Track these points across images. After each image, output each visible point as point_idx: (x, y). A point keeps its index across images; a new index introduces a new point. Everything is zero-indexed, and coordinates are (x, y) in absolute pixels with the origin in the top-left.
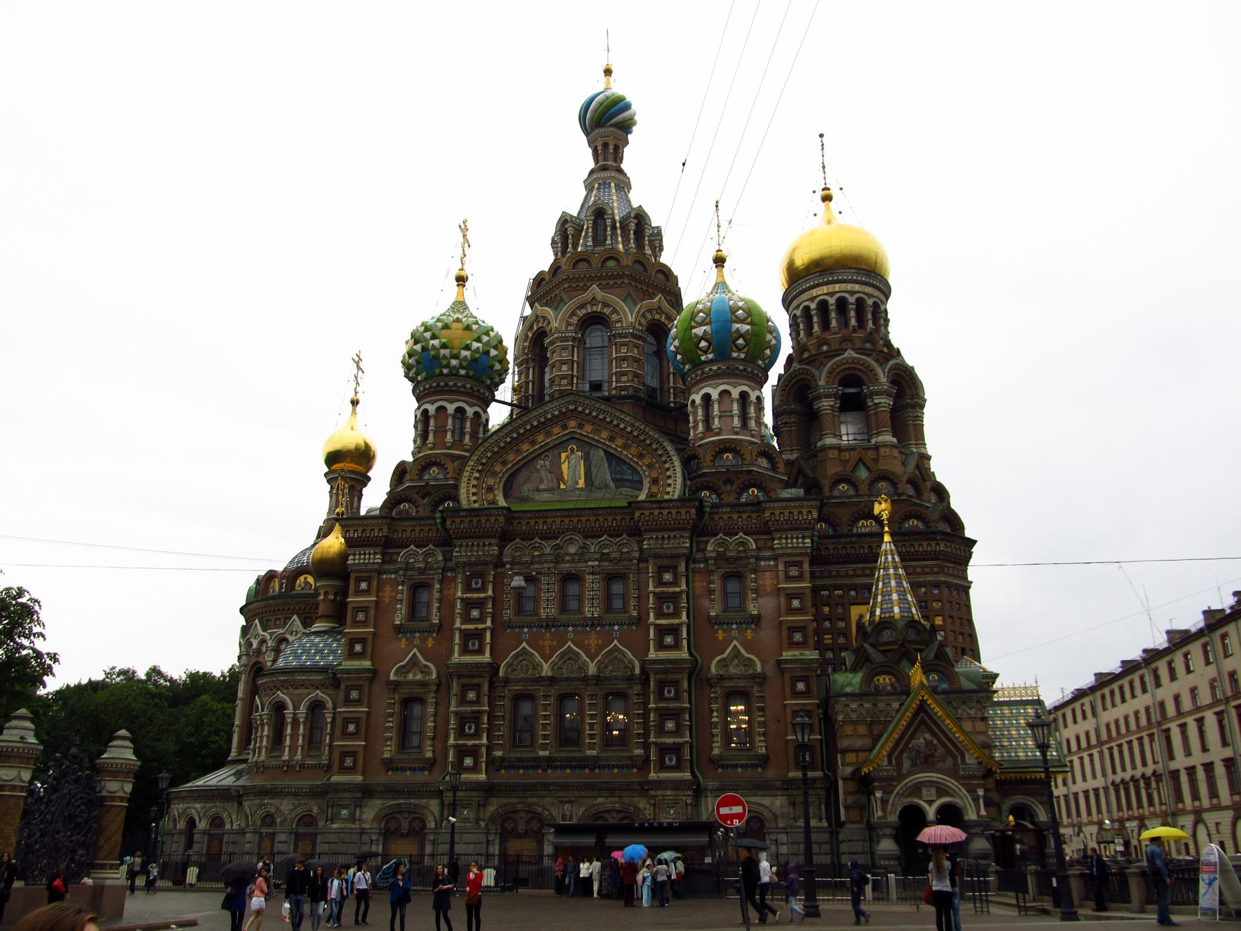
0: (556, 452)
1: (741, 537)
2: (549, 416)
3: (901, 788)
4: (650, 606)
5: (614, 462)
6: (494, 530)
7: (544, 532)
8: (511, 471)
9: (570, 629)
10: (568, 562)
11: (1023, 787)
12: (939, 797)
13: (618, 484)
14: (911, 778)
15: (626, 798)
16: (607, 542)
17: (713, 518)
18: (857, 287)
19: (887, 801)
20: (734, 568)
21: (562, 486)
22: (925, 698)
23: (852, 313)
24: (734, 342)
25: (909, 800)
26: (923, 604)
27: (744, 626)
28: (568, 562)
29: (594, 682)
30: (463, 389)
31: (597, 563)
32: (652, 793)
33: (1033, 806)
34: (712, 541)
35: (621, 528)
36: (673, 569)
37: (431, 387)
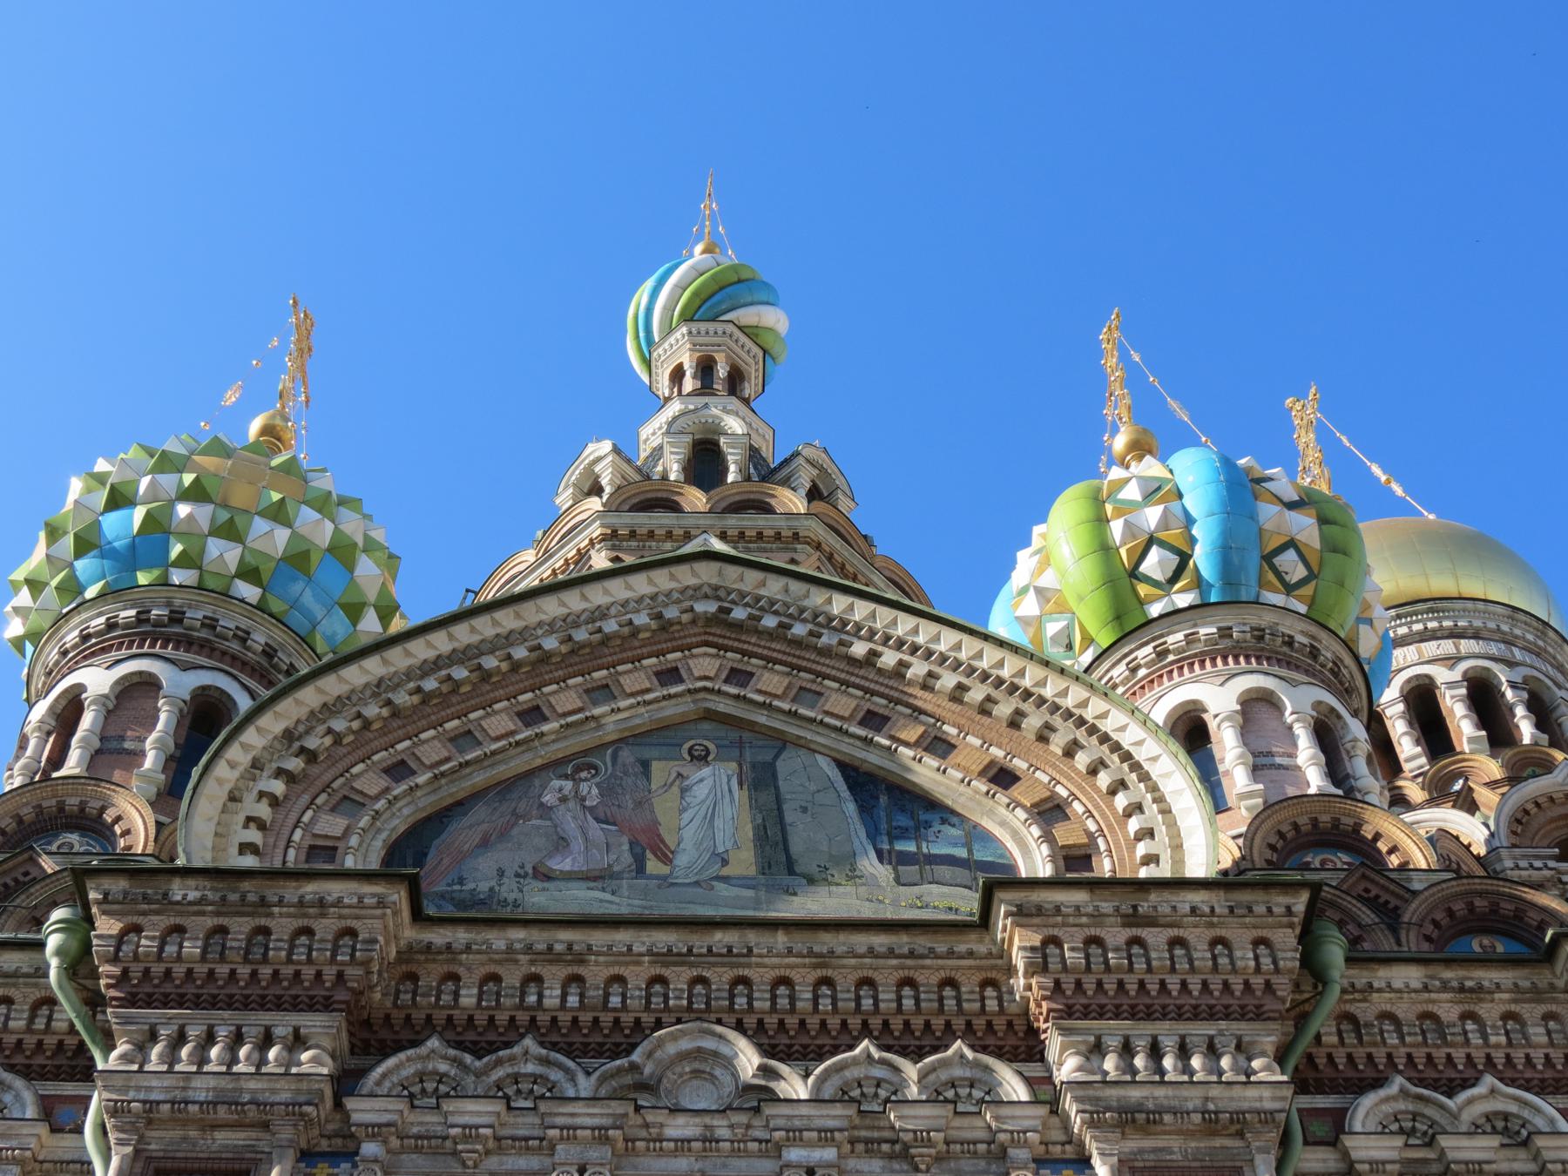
0: (627, 755)
1: (1493, 1091)
2: (610, 626)
5: (883, 800)
6: (330, 973)
7: (564, 1018)
8: (426, 803)
10: (683, 1144)
13: (910, 871)
17: (1351, 1018)
18: (1518, 654)
21: (653, 866)
23: (1520, 711)
24: (1268, 558)
30: (235, 646)
31: (829, 1154)
34: (1368, 1100)
35: (938, 1023)
37: (111, 626)
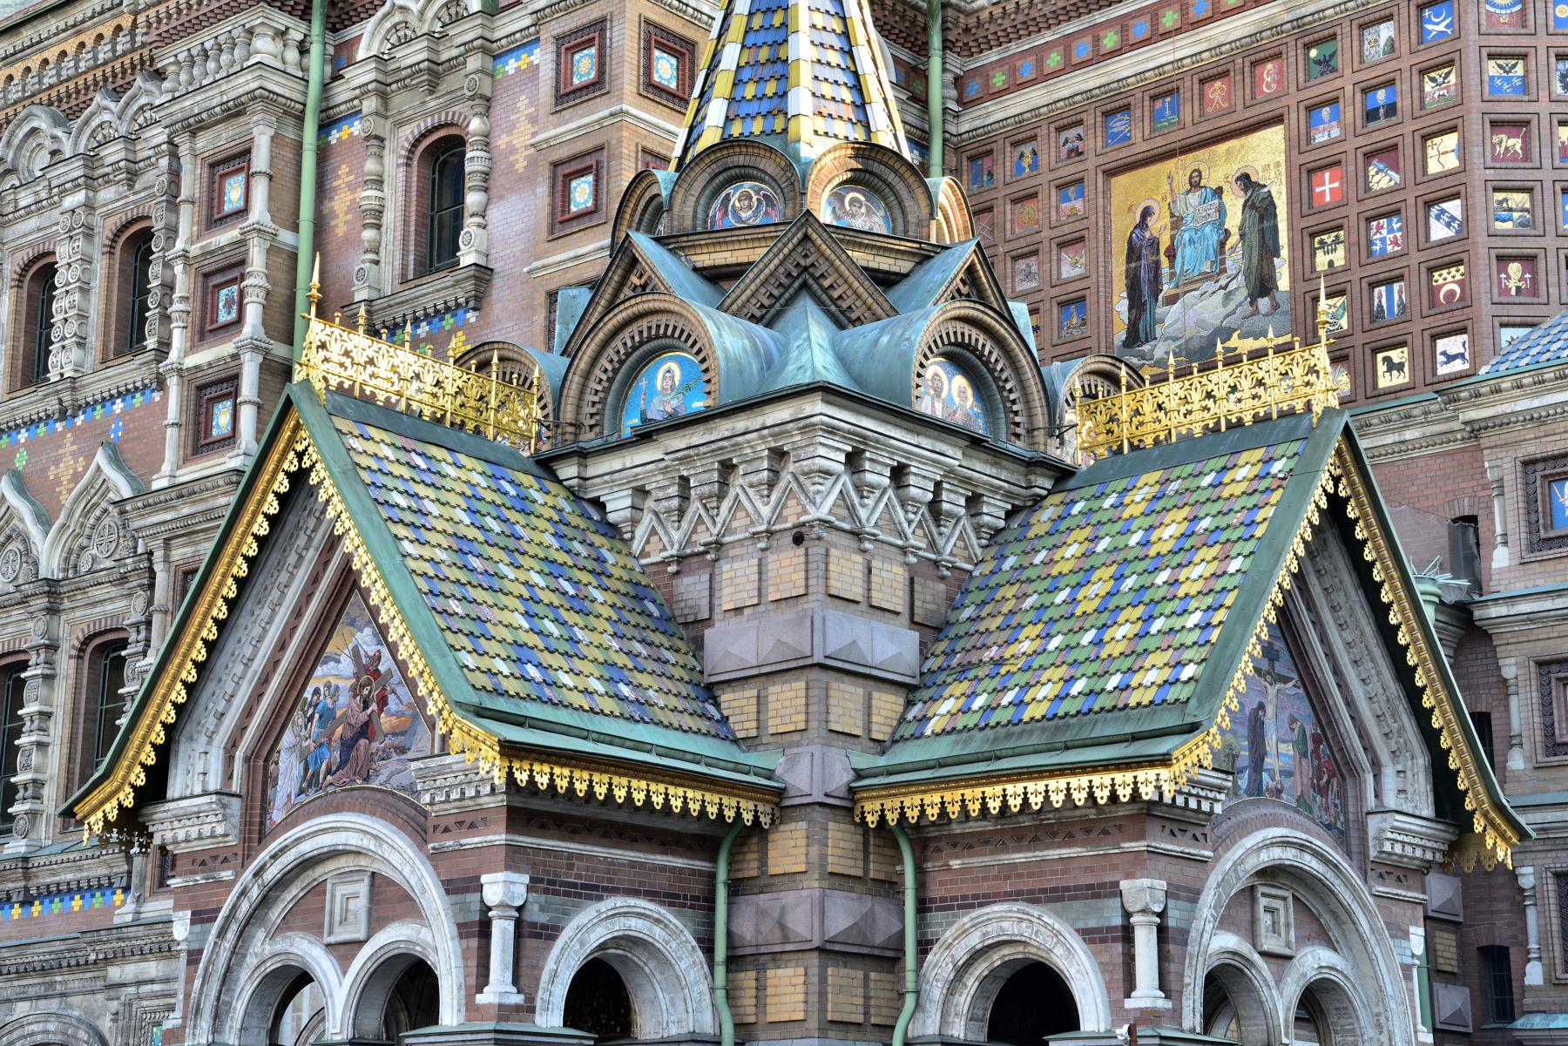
3: (243, 893)
4: (177, 306)
9: (23, 436)
11: (1019, 857)
12: (376, 921)
14: (274, 846)
15: (76, 1000)
16: (106, 117)
19: (200, 952)
20: (438, 110)
22: (307, 463)
25: (281, 945)
26: (1381, 96)
27: (449, 321)
28: (29, 212)
29: (42, 602)
31: (80, 197)
32: (115, 973)
33: (1059, 951)
36: (239, 158)
